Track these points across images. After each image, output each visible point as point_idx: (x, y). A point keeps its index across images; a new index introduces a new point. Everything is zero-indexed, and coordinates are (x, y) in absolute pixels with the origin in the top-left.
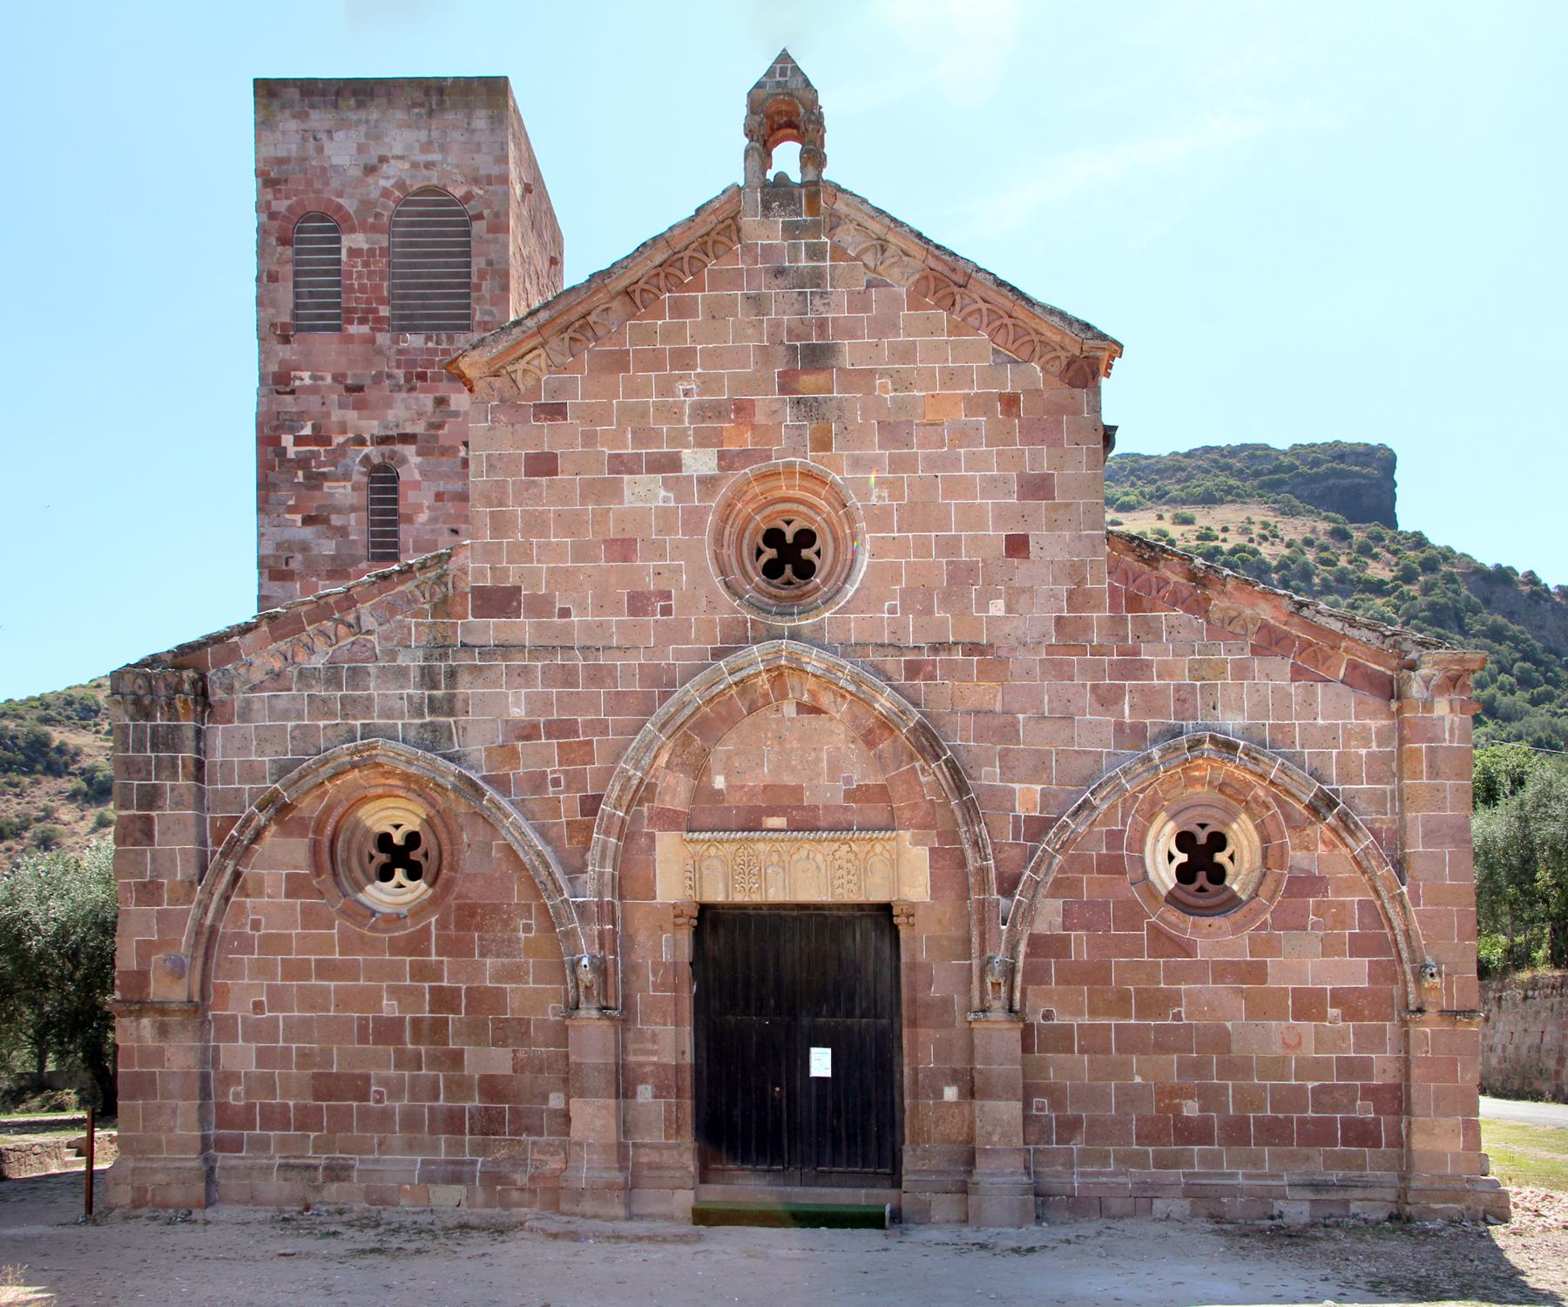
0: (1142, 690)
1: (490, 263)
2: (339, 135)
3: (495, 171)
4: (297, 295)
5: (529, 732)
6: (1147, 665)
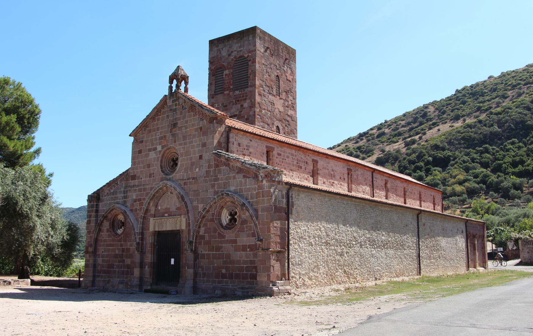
0: (218, 184)
1: (252, 71)
2: (224, 49)
3: (253, 49)
4: (216, 87)
5: (135, 201)
6: (219, 178)
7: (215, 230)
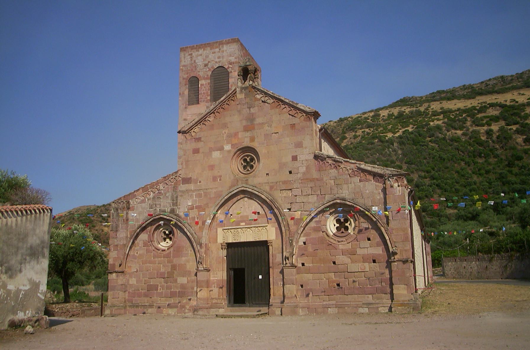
5: (192, 208)
7: (321, 241)
